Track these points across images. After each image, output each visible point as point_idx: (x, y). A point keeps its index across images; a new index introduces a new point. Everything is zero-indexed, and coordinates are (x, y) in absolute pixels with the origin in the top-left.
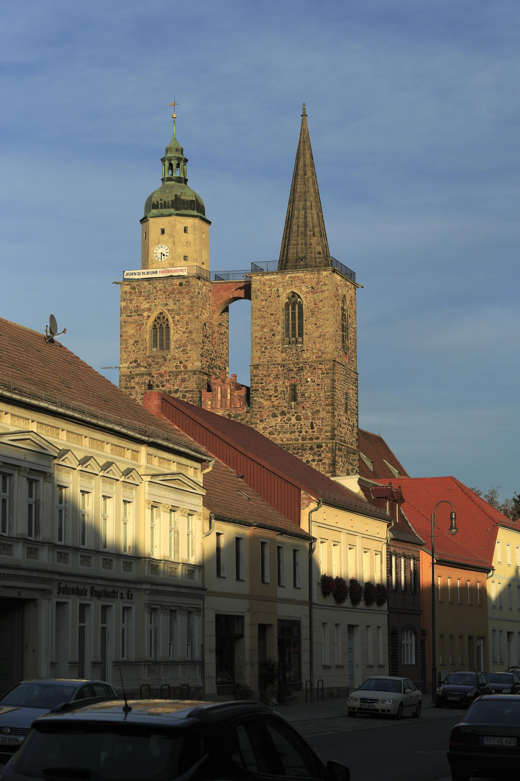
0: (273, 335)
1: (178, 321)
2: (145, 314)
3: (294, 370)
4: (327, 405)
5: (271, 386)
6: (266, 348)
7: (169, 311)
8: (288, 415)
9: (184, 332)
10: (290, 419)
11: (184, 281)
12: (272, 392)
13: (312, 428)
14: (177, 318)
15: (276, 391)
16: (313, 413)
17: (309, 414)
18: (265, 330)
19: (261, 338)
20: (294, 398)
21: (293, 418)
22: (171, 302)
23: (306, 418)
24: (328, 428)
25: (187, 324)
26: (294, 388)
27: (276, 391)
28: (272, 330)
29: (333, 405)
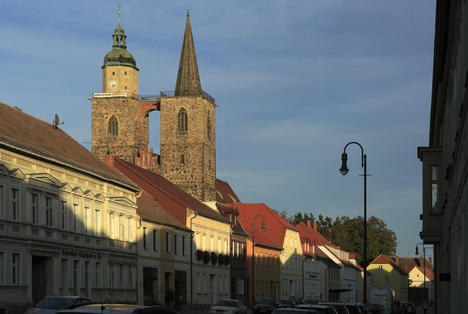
0: (172, 129)
1: (122, 120)
2: (105, 116)
3: (183, 148)
4: (200, 166)
5: (171, 155)
6: (168, 136)
7: (117, 115)
8: (180, 170)
9: (125, 126)
10: (180, 172)
11: (125, 100)
12: (171, 158)
13: (192, 177)
14: (122, 118)
15: (173, 158)
16: (193, 170)
17: (191, 170)
18: (168, 127)
19: (165, 131)
20: (183, 162)
21: (182, 172)
22: (118, 110)
23: (189, 172)
24: (200, 177)
25: (127, 122)
26: (183, 156)
27: (173, 158)
28: (171, 127)
29: (203, 166)
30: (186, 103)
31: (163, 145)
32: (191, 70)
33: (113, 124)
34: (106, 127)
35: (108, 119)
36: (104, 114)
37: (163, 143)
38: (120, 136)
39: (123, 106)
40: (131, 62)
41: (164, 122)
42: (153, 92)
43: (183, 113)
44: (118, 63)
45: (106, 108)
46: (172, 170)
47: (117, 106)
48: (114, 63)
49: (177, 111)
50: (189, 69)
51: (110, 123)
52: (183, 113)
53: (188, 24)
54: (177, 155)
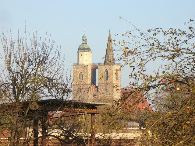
14: (84, 73)
22: (83, 70)
30: (108, 67)
31: (99, 84)
32: (110, 54)
33: (81, 76)
34: (78, 77)
35: (79, 73)
36: (78, 71)
37: (99, 83)
38: (83, 80)
39: (84, 68)
40: (89, 49)
41: (99, 75)
42: (96, 62)
43: (106, 71)
44: (83, 51)
45: (78, 69)
46: (102, 94)
47: (82, 68)
48: (82, 51)
49: (104, 70)
50: (109, 53)
51: (80, 75)
52: (106, 71)
53: (109, 35)
54: (104, 88)
